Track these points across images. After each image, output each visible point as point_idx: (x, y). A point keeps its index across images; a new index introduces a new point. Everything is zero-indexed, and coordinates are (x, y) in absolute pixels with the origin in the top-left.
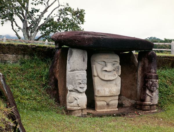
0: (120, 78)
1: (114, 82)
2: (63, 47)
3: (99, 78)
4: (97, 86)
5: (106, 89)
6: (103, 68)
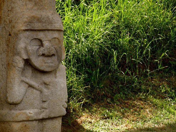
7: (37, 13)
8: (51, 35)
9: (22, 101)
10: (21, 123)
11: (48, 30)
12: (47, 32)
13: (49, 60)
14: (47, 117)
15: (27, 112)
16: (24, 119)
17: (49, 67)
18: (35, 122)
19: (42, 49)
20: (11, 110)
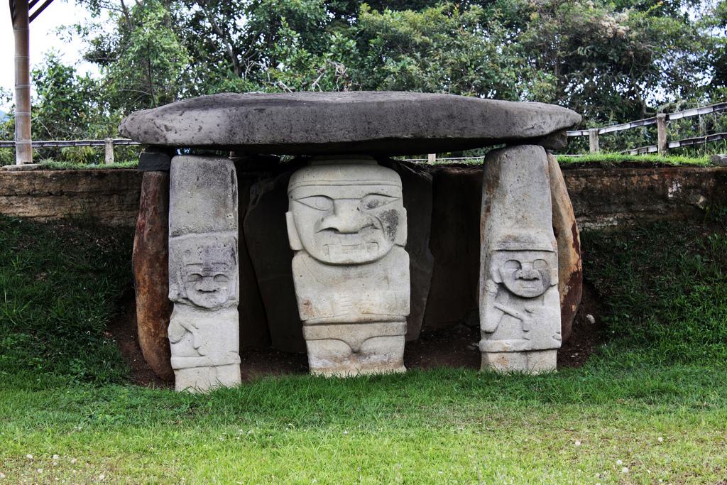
0: (407, 255)
1: (377, 269)
2: (292, 157)
3: (310, 256)
5: (336, 296)
6: (323, 220)
7: (516, 231)
8: (532, 256)
11: (530, 251)
12: (528, 253)
13: (529, 285)
14: (530, 349)
15: (504, 342)
16: (501, 350)
17: (529, 292)
18: (515, 354)
19: (520, 271)
20: (487, 339)
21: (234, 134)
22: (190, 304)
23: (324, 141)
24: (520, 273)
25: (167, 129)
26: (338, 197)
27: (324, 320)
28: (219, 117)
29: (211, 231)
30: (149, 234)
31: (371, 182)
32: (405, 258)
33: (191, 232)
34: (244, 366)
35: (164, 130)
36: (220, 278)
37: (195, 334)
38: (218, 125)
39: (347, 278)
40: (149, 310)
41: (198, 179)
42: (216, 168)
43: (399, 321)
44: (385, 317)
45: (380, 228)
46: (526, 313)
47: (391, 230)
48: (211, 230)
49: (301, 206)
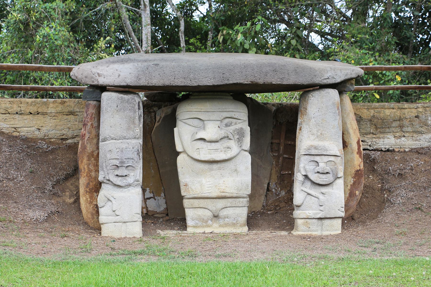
3: (188, 155)
4: (184, 174)
5: (204, 181)
6: (197, 133)
7: (316, 143)
9: (303, 203)
10: (303, 220)
12: (323, 156)
15: (307, 212)
18: (314, 220)
19: (318, 168)
21: (140, 79)
22: (111, 183)
23: (195, 84)
24: (318, 169)
25: (99, 75)
26: (207, 119)
27: (196, 196)
28: (130, 69)
29: (125, 139)
30: (87, 140)
31: (228, 110)
32: (248, 158)
33: (112, 139)
34: (144, 224)
35: (97, 76)
36: (130, 168)
37: (114, 202)
38: (130, 74)
39: (212, 170)
40: (87, 187)
41: (117, 107)
42: (128, 100)
43: (243, 198)
44: (235, 195)
45: (233, 139)
46: (322, 195)
47: (240, 140)
48: (125, 138)
49: (183, 124)
